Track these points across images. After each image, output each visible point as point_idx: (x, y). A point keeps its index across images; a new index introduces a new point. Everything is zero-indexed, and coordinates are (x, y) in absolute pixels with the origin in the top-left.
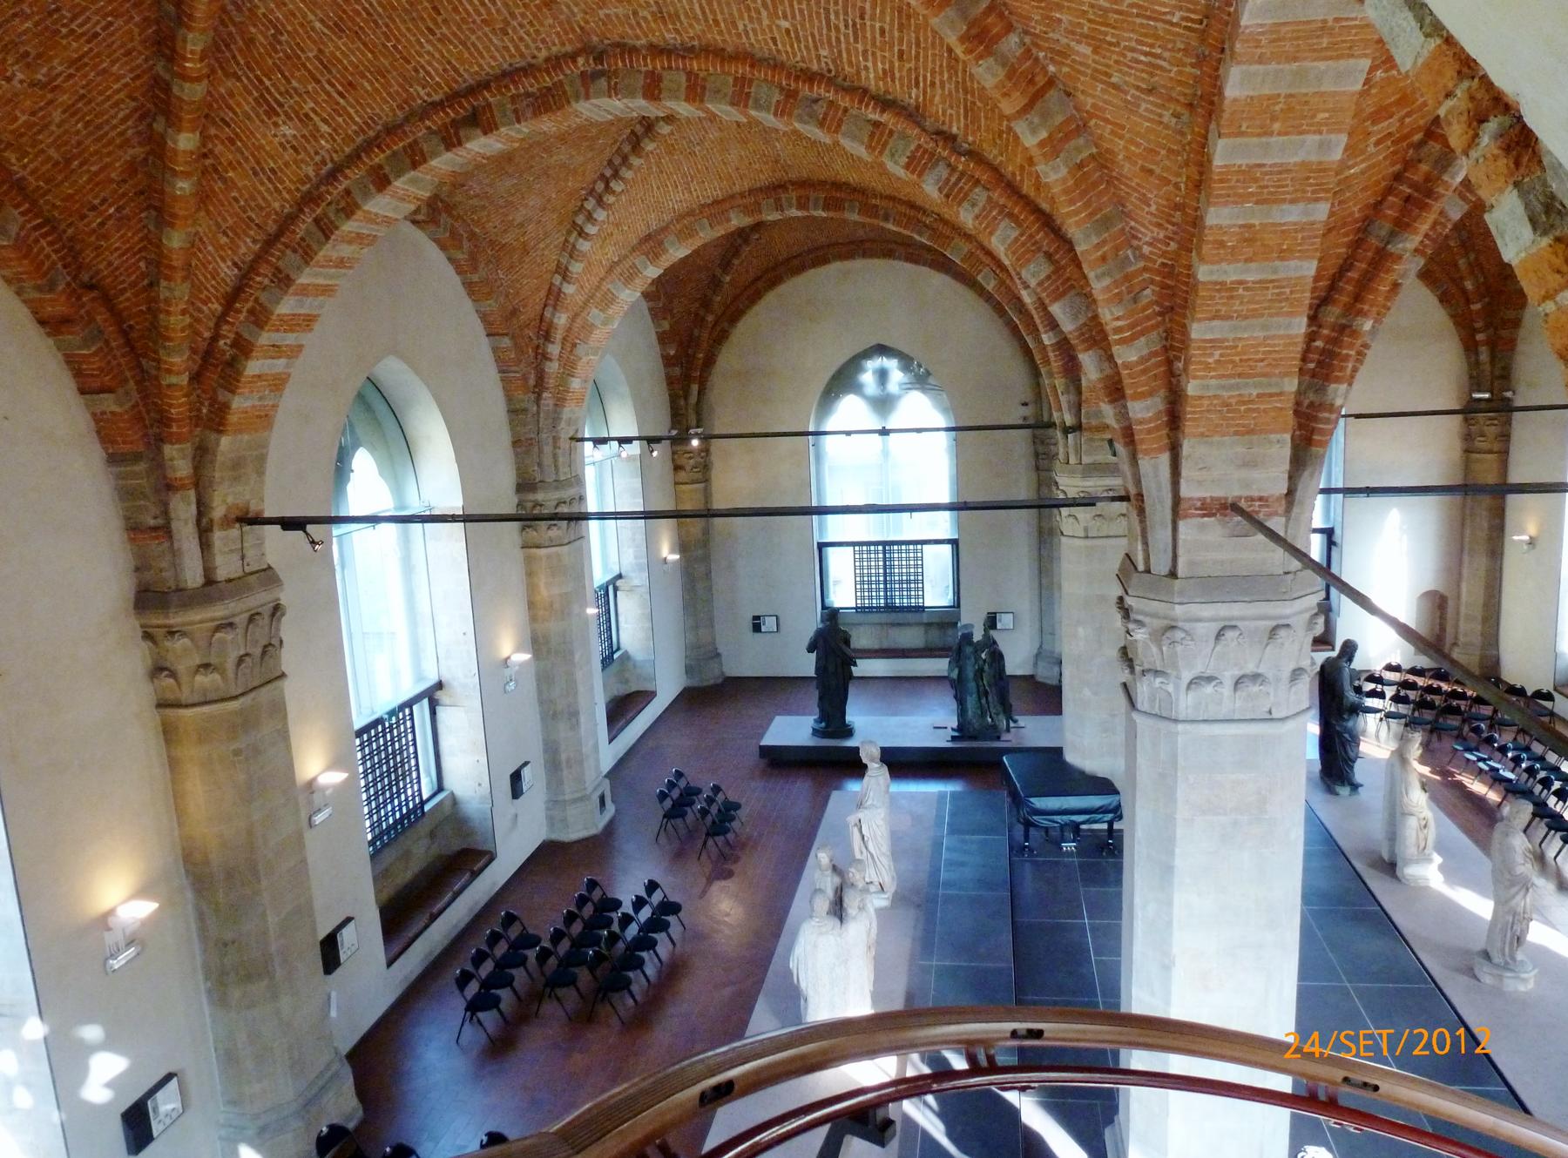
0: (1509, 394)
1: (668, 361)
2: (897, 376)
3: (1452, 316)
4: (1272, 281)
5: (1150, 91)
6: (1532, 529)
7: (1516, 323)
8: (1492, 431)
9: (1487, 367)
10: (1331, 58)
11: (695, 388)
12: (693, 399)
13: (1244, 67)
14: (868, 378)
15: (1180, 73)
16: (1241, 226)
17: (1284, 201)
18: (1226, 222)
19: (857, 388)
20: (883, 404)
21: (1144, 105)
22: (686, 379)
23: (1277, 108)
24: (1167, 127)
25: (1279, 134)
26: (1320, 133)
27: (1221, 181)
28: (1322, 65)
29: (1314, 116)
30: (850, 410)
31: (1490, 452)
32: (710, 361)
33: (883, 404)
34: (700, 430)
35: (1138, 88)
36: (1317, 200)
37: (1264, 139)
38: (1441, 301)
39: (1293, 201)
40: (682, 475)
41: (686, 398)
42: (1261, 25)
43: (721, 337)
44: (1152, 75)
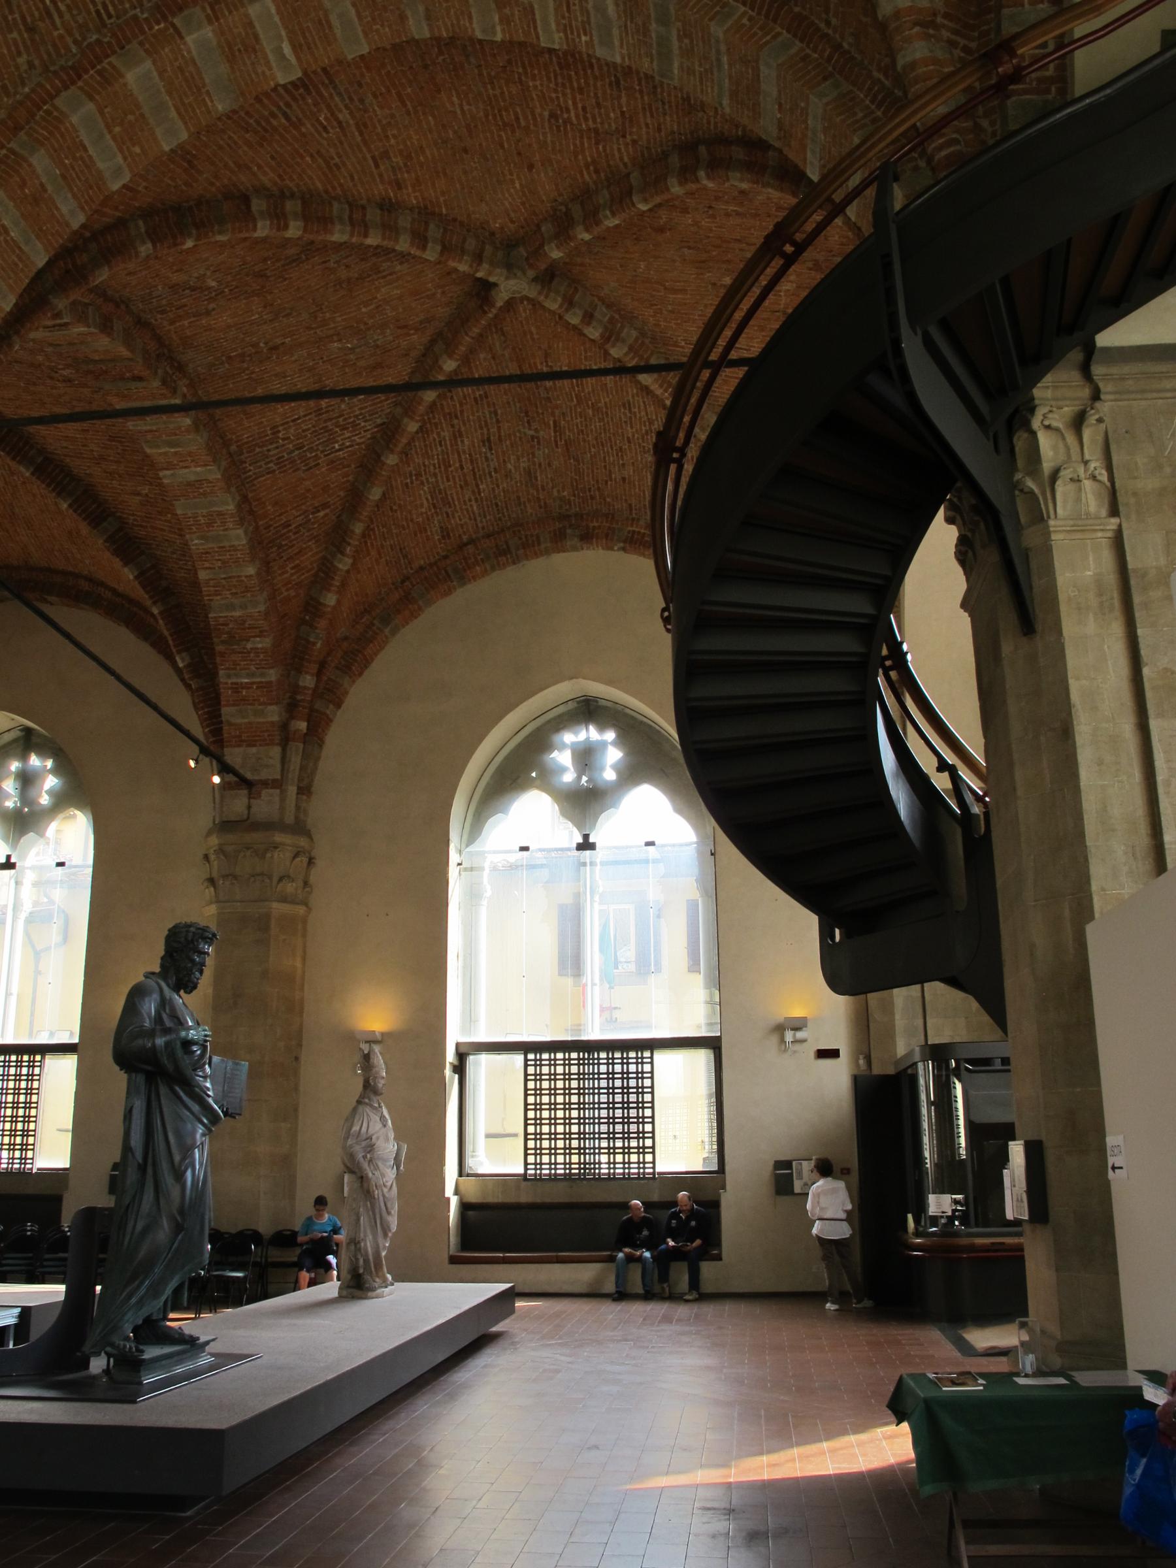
4: (20, 248)
5: (31, 30)
10: (179, 114)
13: (153, 68)
15: (61, 37)
16: (42, 185)
17: (71, 190)
18: (39, 170)
21: (15, 35)
23: (130, 117)
24: (17, 67)
25: (114, 138)
26: (125, 159)
27: (62, 135)
28: (173, 114)
29: (134, 145)
35: (23, 18)
36: (82, 208)
37: (105, 131)
39: (75, 196)
42: (189, 52)
44: (42, 19)
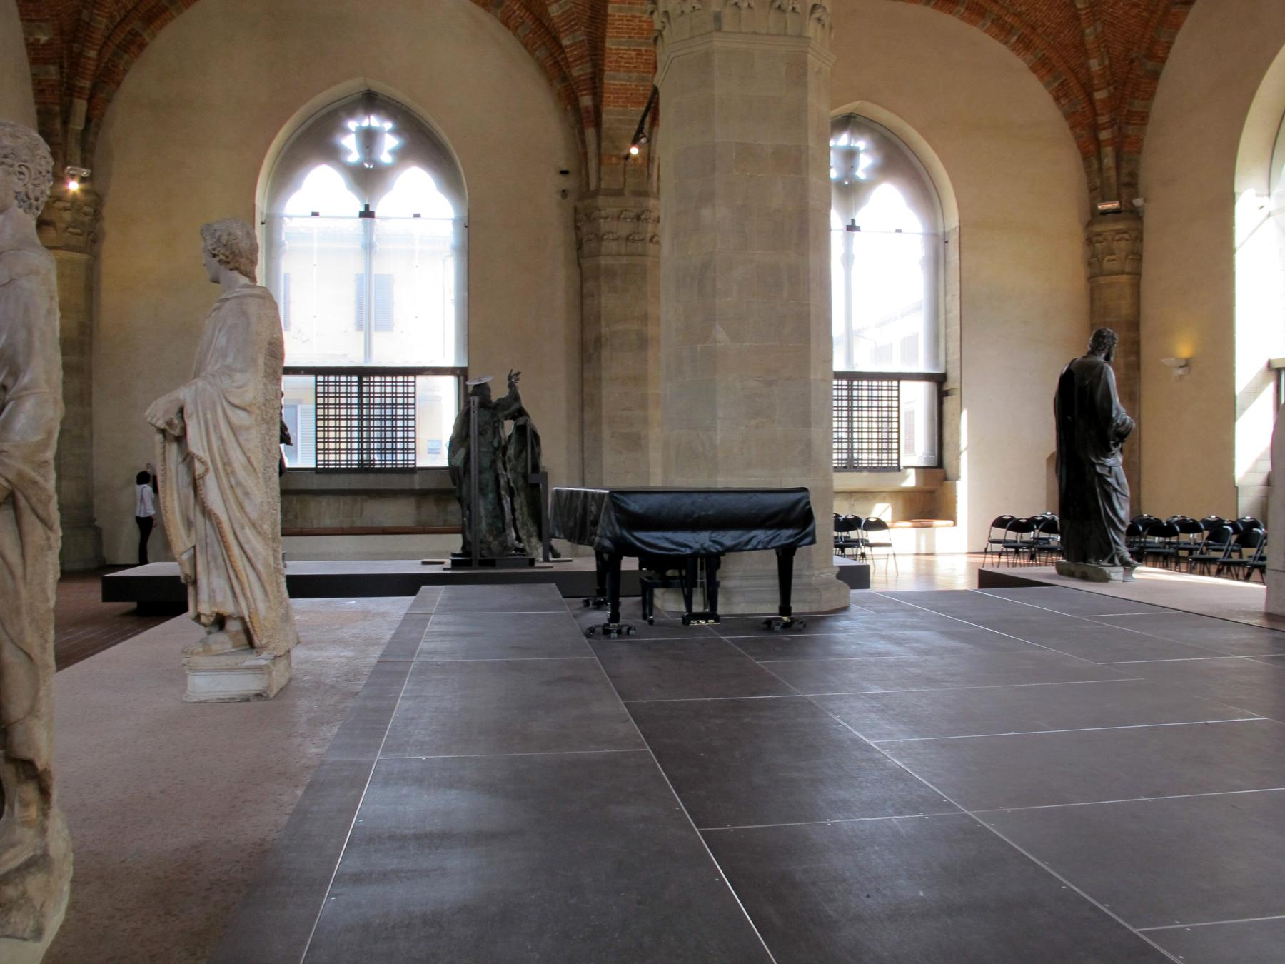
0: (1138, 202)
1: (36, 54)
2: (390, 143)
3: (1067, 116)
6: (1184, 350)
7: (1143, 118)
8: (1122, 246)
9: (1113, 173)
11: (81, 106)
12: (78, 124)
14: (349, 143)
19: (332, 154)
20: (367, 178)
22: (70, 90)
30: (320, 193)
31: (1122, 273)
32: (108, 77)
33: (367, 178)
34: (85, 173)
38: (1057, 99)
40: (51, 233)
41: (65, 123)
43: (134, 45)
